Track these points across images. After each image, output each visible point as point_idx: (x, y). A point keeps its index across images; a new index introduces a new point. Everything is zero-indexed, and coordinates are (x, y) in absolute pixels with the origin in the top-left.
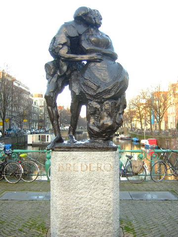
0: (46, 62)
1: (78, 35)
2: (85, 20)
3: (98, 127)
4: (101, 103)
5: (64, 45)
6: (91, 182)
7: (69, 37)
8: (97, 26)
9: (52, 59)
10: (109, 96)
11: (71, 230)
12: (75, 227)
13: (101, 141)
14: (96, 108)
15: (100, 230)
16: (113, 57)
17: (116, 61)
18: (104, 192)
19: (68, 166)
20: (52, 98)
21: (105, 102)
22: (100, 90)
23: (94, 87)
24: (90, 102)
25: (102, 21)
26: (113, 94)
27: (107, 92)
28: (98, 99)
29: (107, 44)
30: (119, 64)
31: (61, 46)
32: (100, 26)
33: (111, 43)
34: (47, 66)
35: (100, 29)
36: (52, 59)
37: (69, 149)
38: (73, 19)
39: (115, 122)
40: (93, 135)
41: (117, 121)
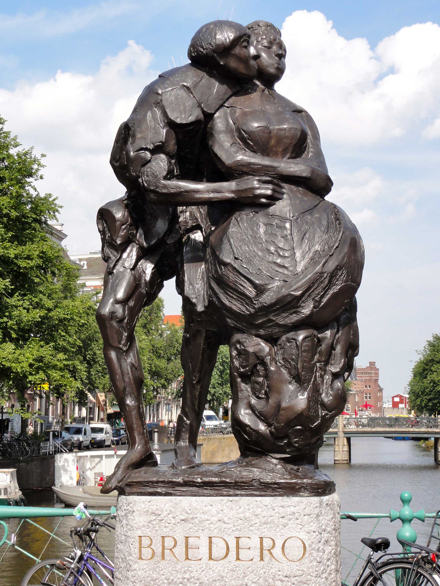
0: (101, 204)
1: (202, 116)
2: (224, 66)
3: (261, 416)
4: (272, 340)
5: (156, 150)
7: (171, 125)
10: (295, 318)
13: (275, 461)
16: (317, 185)
17: (327, 198)
21: (284, 338)
22: (267, 298)
23: (251, 292)
24: (238, 336)
25: (288, 61)
26: (307, 309)
27: (289, 304)
29: (301, 140)
32: (280, 71)
34: (104, 215)
36: (120, 191)
37: (171, 488)
38: (190, 62)
39: (315, 398)
40: (252, 446)
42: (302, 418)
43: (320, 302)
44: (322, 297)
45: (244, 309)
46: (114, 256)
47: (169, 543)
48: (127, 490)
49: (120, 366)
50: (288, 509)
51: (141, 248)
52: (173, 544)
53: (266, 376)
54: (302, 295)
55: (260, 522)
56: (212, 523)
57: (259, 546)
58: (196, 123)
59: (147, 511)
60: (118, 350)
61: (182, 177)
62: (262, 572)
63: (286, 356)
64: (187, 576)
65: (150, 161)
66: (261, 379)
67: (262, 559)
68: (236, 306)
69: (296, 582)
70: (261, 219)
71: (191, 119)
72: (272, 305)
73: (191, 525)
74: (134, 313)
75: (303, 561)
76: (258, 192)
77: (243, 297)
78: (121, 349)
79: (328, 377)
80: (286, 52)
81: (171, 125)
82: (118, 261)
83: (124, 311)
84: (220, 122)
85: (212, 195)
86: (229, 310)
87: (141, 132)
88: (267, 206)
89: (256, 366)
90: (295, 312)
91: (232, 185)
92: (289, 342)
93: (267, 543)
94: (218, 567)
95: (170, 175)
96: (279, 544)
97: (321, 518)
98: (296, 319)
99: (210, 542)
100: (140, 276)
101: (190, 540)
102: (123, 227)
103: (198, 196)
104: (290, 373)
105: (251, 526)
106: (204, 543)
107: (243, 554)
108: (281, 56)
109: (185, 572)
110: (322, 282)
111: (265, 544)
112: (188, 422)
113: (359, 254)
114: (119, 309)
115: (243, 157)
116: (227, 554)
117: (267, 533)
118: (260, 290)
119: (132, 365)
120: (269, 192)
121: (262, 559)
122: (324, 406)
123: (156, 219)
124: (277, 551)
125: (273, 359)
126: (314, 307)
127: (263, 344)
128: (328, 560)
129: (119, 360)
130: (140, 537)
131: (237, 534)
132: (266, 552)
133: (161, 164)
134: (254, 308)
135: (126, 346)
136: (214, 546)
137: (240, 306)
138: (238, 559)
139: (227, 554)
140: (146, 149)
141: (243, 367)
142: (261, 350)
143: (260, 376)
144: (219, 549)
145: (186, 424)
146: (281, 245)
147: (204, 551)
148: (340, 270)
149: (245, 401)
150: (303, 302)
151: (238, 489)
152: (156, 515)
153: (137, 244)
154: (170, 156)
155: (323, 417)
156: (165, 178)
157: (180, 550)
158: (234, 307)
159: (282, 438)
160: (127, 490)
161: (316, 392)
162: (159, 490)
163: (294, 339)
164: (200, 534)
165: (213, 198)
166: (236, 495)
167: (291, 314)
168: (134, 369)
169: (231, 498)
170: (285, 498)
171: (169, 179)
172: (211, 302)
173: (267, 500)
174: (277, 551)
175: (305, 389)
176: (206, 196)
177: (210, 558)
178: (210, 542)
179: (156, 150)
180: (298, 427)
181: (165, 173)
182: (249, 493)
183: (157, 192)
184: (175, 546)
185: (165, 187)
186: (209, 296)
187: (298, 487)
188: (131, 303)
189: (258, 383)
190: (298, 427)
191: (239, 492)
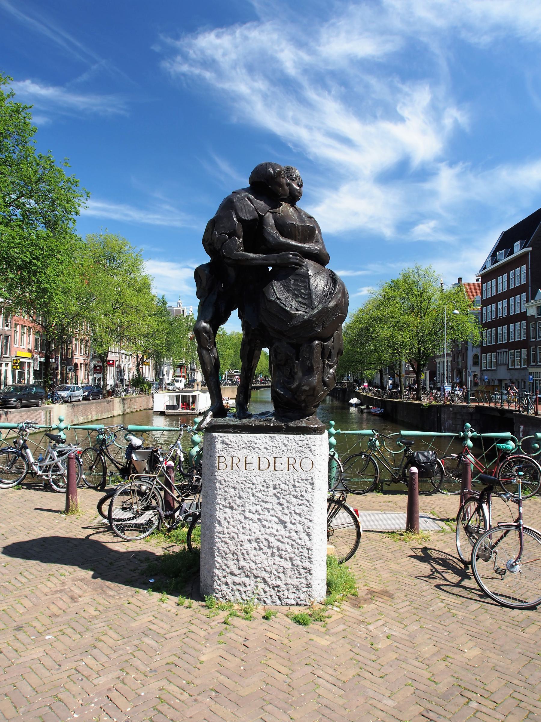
8: (293, 198)
9: (207, 259)
11: (236, 579)
22: (296, 322)
35: (298, 204)
47: (235, 460)
58: (254, 220)
61: (245, 252)
62: (288, 477)
71: (251, 218)
75: (311, 471)
76: (291, 260)
93: (292, 461)
96: (298, 461)
97: (321, 447)
103: (255, 262)
108: (301, 186)
122: (325, 384)
124: (297, 466)
131: (275, 456)
132: (291, 467)
146: (302, 291)
157: (242, 465)
164: (254, 455)
170: (302, 436)
173: (291, 436)
174: (297, 466)
176: (260, 262)
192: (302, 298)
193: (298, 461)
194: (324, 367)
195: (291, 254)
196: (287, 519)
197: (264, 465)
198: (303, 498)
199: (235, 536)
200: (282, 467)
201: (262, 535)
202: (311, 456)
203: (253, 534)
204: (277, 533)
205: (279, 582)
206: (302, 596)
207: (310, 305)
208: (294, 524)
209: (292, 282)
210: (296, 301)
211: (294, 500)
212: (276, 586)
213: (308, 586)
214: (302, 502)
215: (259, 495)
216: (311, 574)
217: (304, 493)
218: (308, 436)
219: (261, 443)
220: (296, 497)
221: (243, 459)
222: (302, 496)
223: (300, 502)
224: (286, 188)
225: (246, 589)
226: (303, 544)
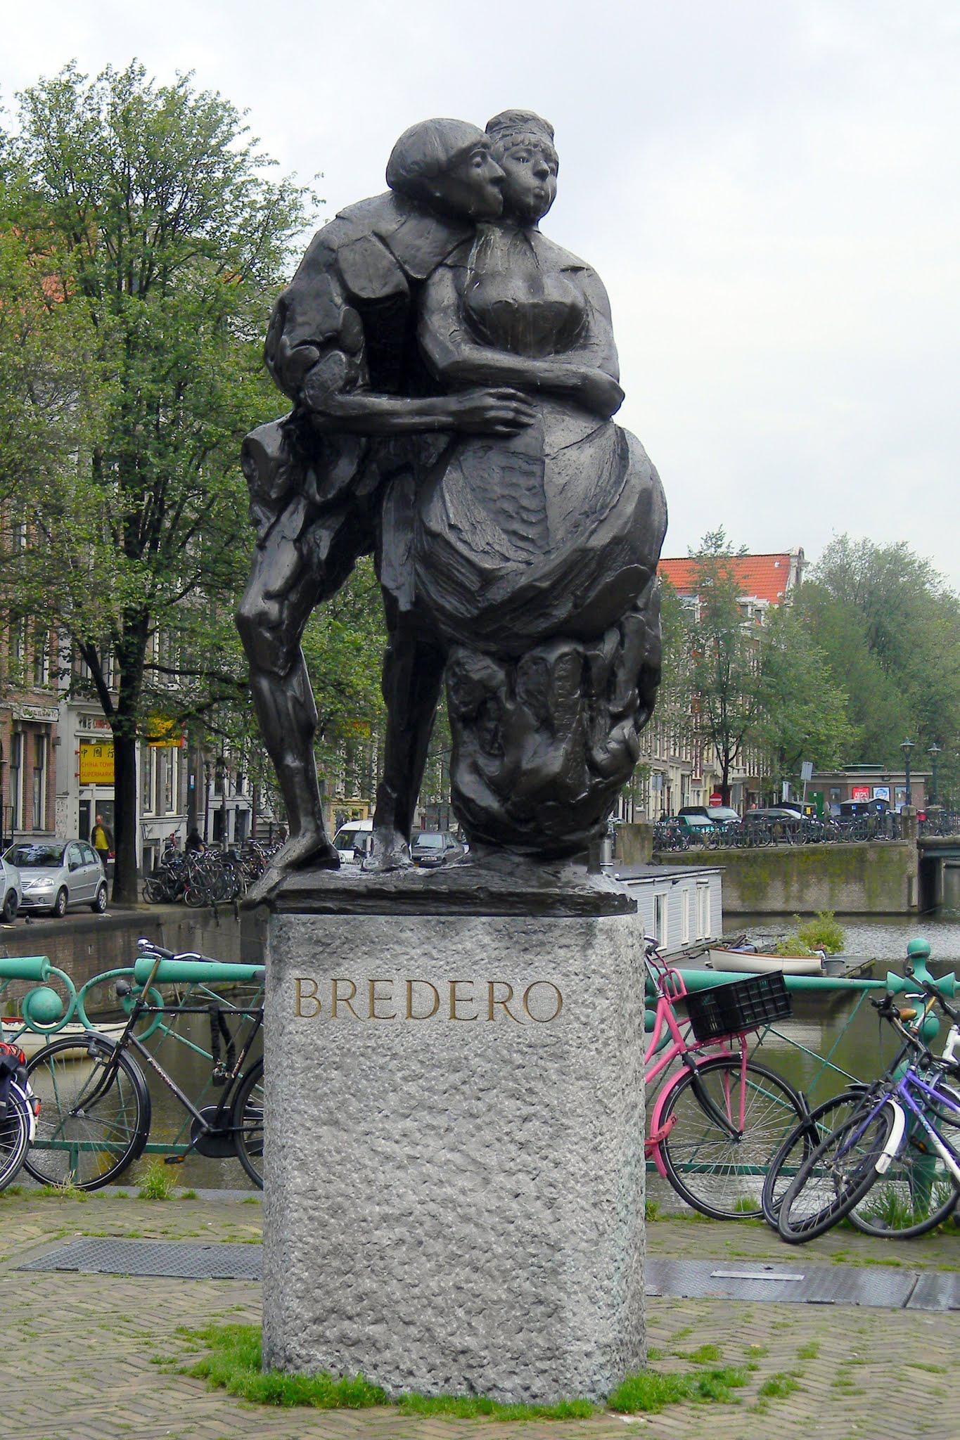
3: (495, 786)
4: (509, 660)
5: (330, 342)
6: (456, 1078)
7: (352, 299)
8: (522, 213)
10: (543, 625)
12: (371, 1316)
13: (517, 859)
14: (483, 685)
15: (501, 1340)
16: (596, 401)
18: (520, 1136)
19: (344, 989)
20: (274, 627)
21: (527, 657)
22: (498, 594)
23: (473, 583)
26: (562, 611)
27: (530, 600)
28: (488, 638)
30: (621, 433)
31: (315, 352)
32: (544, 202)
33: (607, 314)
35: (547, 226)
41: (600, 756)
42: (554, 787)
43: (584, 597)
44: (587, 589)
45: (463, 609)
46: (268, 519)
48: (279, 904)
49: (275, 701)
50: (534, 937)
51: (311, 504)
52: (350, 991)
53: (499, 720)
54: (553, 586)
55: (489, 957)
56: (412, 958)
57: (486, 996)
58: (397, 296)
59: (310, 938)
60: (271, 675)
61: (375, 387)
62: (491, 1037)
63: (531, 687)
64: (372, 1043)
65: (315, 364)
66: (491, 725)
67: (491, 1018)
68: (450, 603)
69: (545, 1055)
70: (496, 459)
71: (387, 290)
72: (503, 604)
73: (378, 962)
74: (299, 616)
75: (556, 1021)
76: (493, 414)
77: (462, 591)
78: (276, 674)
79: (602, 722)
80: (557, 164)
81: (352, 299)
82: (272, 527)
83: (281, 612)
84: (443, 291)
85: (417, 420)
86: (441, 609)
87: (304, 314)
88: (508, 437)
89: (484, 702)
90: (542, 615)
91: (452, 403)
92: (535, 664)
94: (423, 1030)
95: (349, 385)
96: (519, 991)
98: (544, 625)
99: (410, 990)
100: (311, 552)
101: (378, 985)
102: (282, 470)
104: (537, 715)
105: (475, 963)
106: (399, 989)
107: (463, 1009)
109: (369, 1037)
110: (586, 565)
111: (496, 993)
112: (394, 795)
113: (656, 518)
114: (273, 608)
115: (472, 353)
116: (435, 1009)
117: (499, 976)
118: (488, 578)
119: (296, 700)
120: (510, 415)
121: (491, 1018)
122: (595, 768)
123: (338, 454)
125: (512, 694)
126: (575, 606)
127: (495, 668)
128: (603, 1021)
129: (272, 693)
130: (298, 979)
133: (336, 365)
134: (477, 608)
135: (283, 668)
136: (415, 996)
137: (458, 605)
138: (453, 1017)
139: (435, 1009)
140: (312, 343)
141: (465, 704)
142: (491, 677)
143: (490, 720)
144: (423, 1002)
145: (391, 798)
146: (525, 502)
147: (399, 1003)
148: (617, 544)
149: (469, 761)
150: (556, 598)
151: (455, 904)
152: (323, 944)
153: (306, 498)
154: (351, 353)
155: (594, 789)
156: (342, 391)
157: (361, 1002)
158: (447, 606)
159: (527, 821)
160: (279, 904)
161: (584, 746)
162: (329, 905)
163: (542, 659)
165: (421, 424)
166: (451, 914)
167: (536, 618)
168: (298, 707)
169: (443, 918)
170: (529, 920)
171: (349, 392)
172: (418, 597)
174: (516, 1005)
175: (562, 740)
177: (410, 1015)
178: (410, 990)
179: (330, 342)
180: (550, 803)
181: (341, 383)
182: (472, 910)
183: (329, 415)
184: (352, 996)
185: (342, 405)
186: (417, 587)
187: (550, 901)
188: (293, 597)
189: (488, 730)
190: (550, 803)
191: (455, 909)
192: (524, 521)
193: (519, 991)
194: (592, 720)
195: (491, 395)
196: (492, 1159)
197: (423, 1002)
198: (535, 1100)
199: (347, 1204)
200: (474, 1008)
201: (422, 1203)
202: (557, 979)
203: (395, 1200)
204: (461, 1198)
205: (469, 1341)
206: (538, 1385)
207: (542, 543)
208: (510, 1173)
209: (497, 476)
210: (506, 531)
211: (510, 1104)
212: (463, 1352)
213: (553, 1353)
214: (531, 1110)
215: (411, 1088)
216: (561, 1320)
217: (538, 1086)
218: (547, 920)
219: (414, 940)
220: (515, 1095)
221: (363, 985)
222: (530, 1091)
223: (527, 1110)
224: (494, 191)
225: (377, 1358)
226: (537, 1230)
